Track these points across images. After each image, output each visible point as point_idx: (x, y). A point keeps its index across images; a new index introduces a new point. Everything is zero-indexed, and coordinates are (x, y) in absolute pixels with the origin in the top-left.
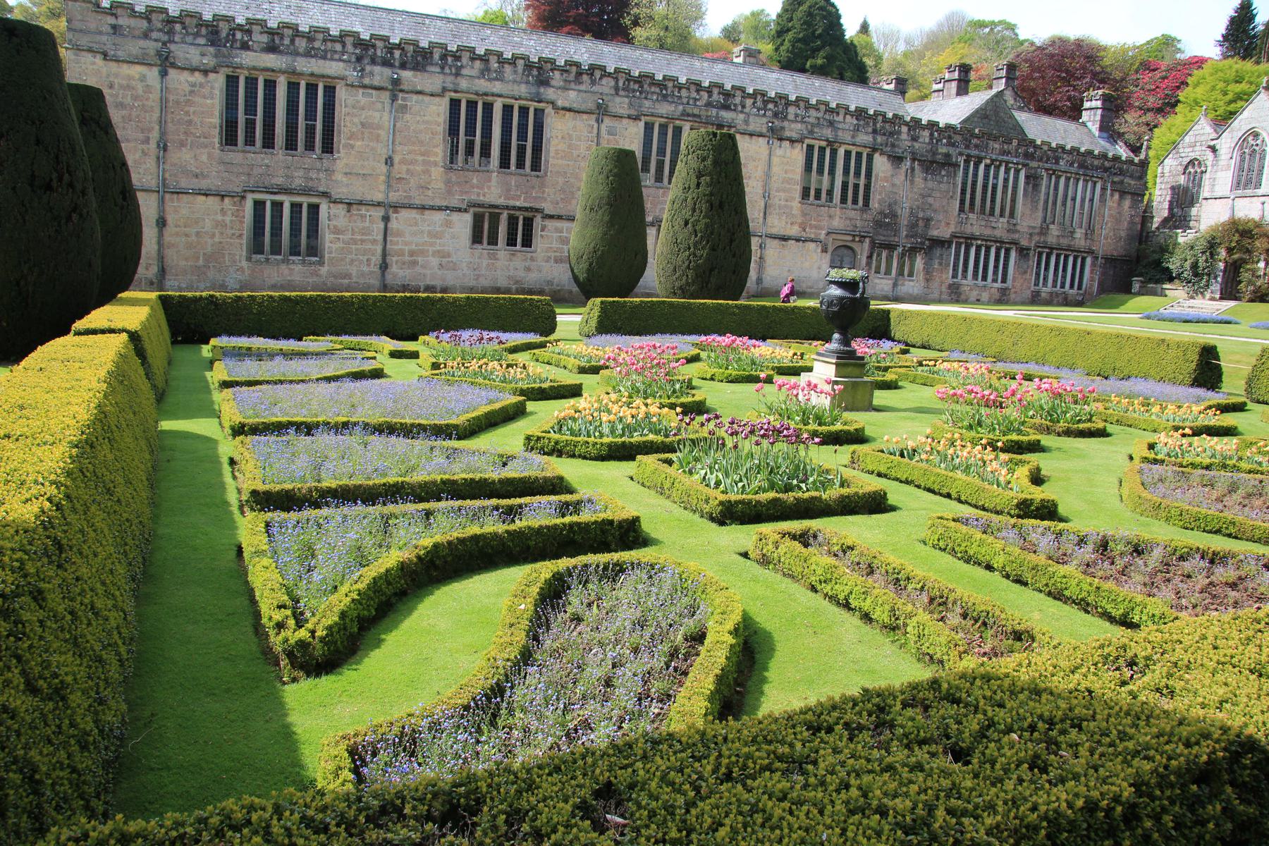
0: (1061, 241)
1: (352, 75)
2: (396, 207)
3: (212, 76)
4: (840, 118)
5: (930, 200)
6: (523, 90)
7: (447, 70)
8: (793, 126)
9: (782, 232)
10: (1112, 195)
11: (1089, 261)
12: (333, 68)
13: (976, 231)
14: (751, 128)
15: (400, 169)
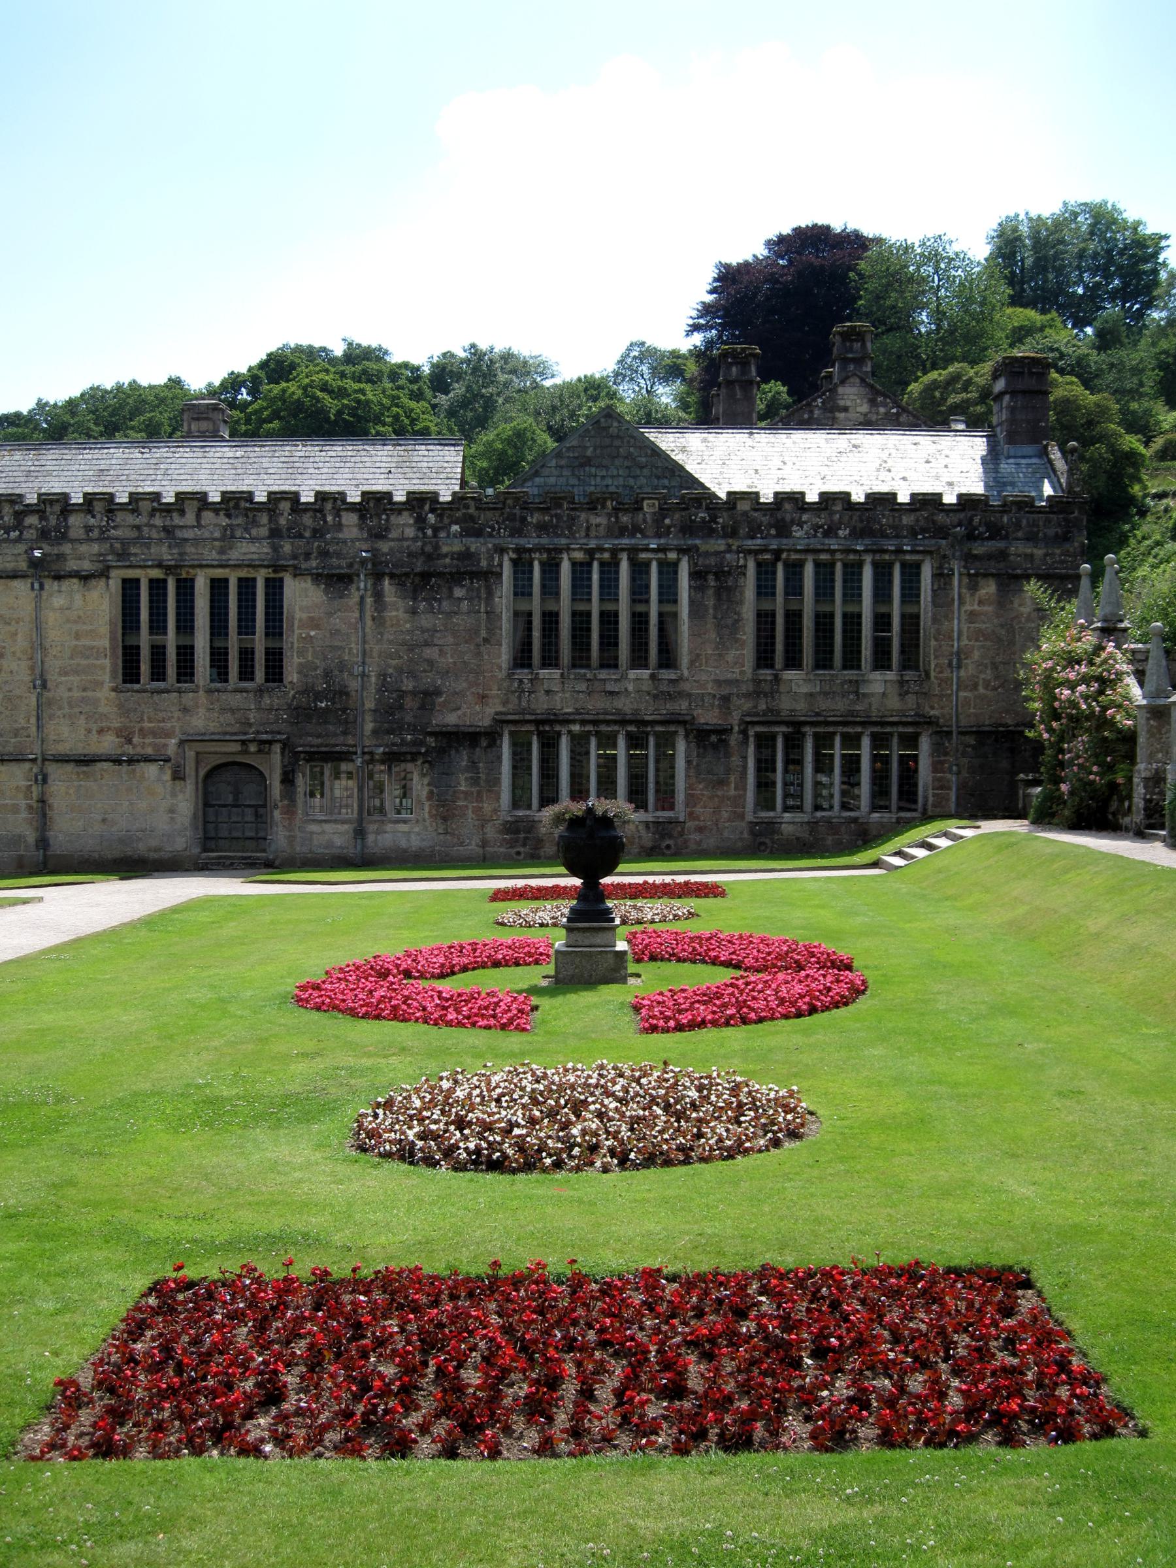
0: (823, 704)
4: (190, 518)
5: (428, 652)
8: (84, 548)
9: (80, 750)
10: (973, 588)
11: (925, 744)
13: (564, 703)
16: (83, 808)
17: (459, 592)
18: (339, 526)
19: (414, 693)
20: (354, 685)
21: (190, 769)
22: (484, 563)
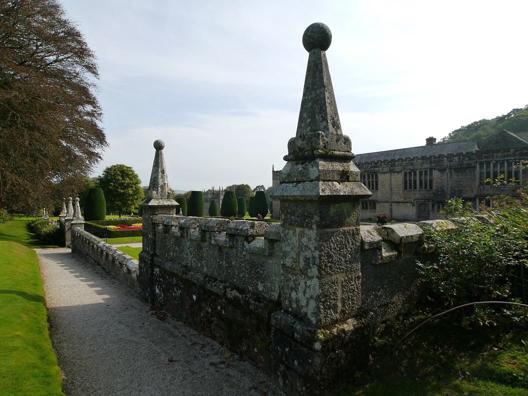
4: (416, 161)
5: (461, 183)
8: (397, 168)
17: (467, 171)
18: (443, 161)
19: (458, 191)
20: (446, 189)
21: (415, 204)
22: (473, 165)
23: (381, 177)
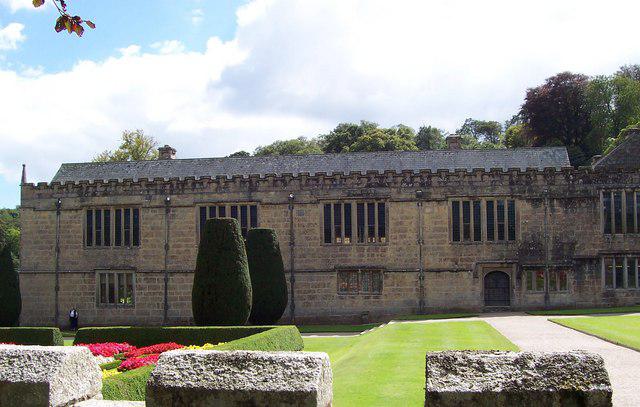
1: (144, 201)
2: (173, 273)
3: (79, 212)
6: (242, 196)
7: (195, 191)
12: (136, 199)
14: (403, 196)
15: (172, 251)
16: (437, 290)
17: (583, 205)
23: (394, 212)
